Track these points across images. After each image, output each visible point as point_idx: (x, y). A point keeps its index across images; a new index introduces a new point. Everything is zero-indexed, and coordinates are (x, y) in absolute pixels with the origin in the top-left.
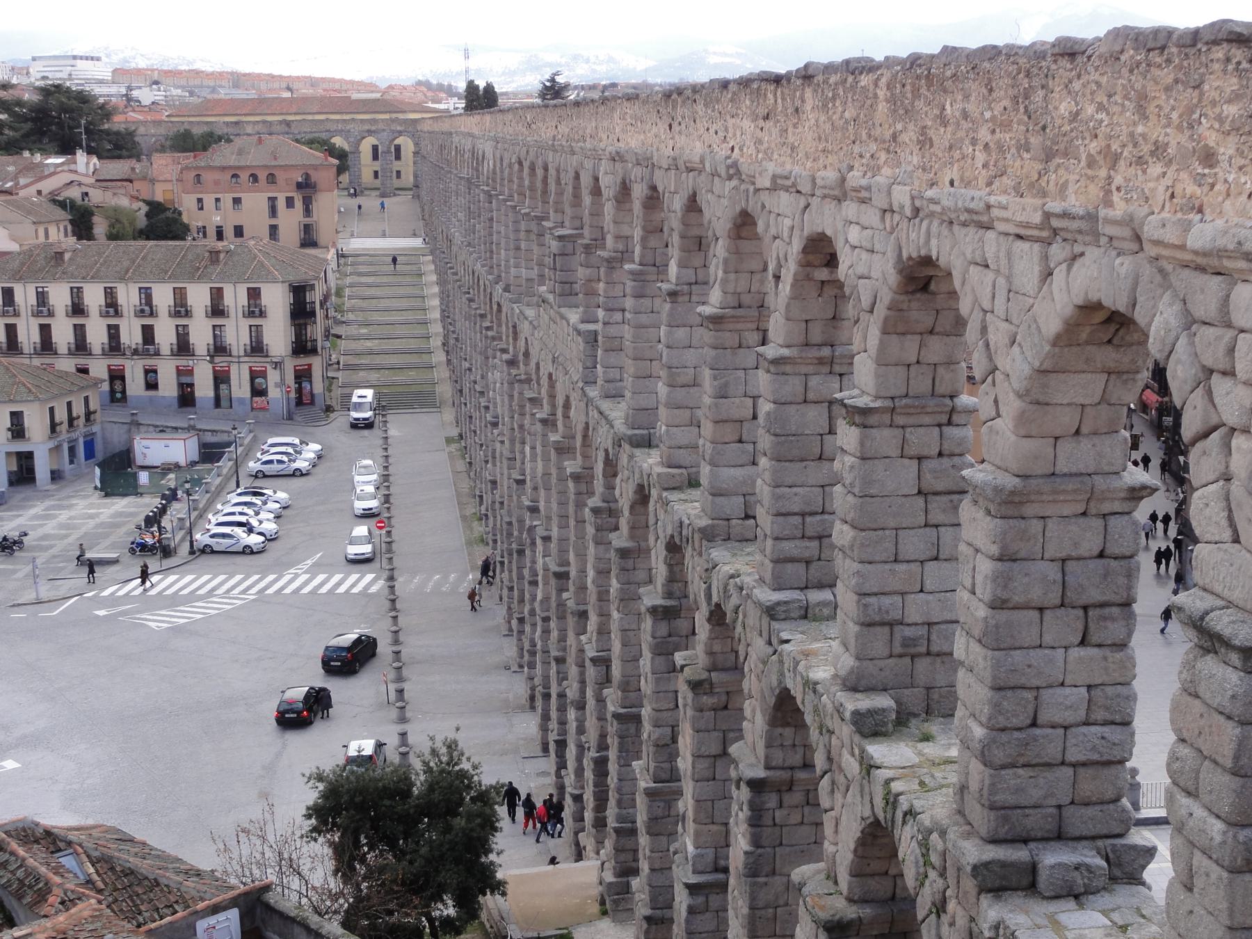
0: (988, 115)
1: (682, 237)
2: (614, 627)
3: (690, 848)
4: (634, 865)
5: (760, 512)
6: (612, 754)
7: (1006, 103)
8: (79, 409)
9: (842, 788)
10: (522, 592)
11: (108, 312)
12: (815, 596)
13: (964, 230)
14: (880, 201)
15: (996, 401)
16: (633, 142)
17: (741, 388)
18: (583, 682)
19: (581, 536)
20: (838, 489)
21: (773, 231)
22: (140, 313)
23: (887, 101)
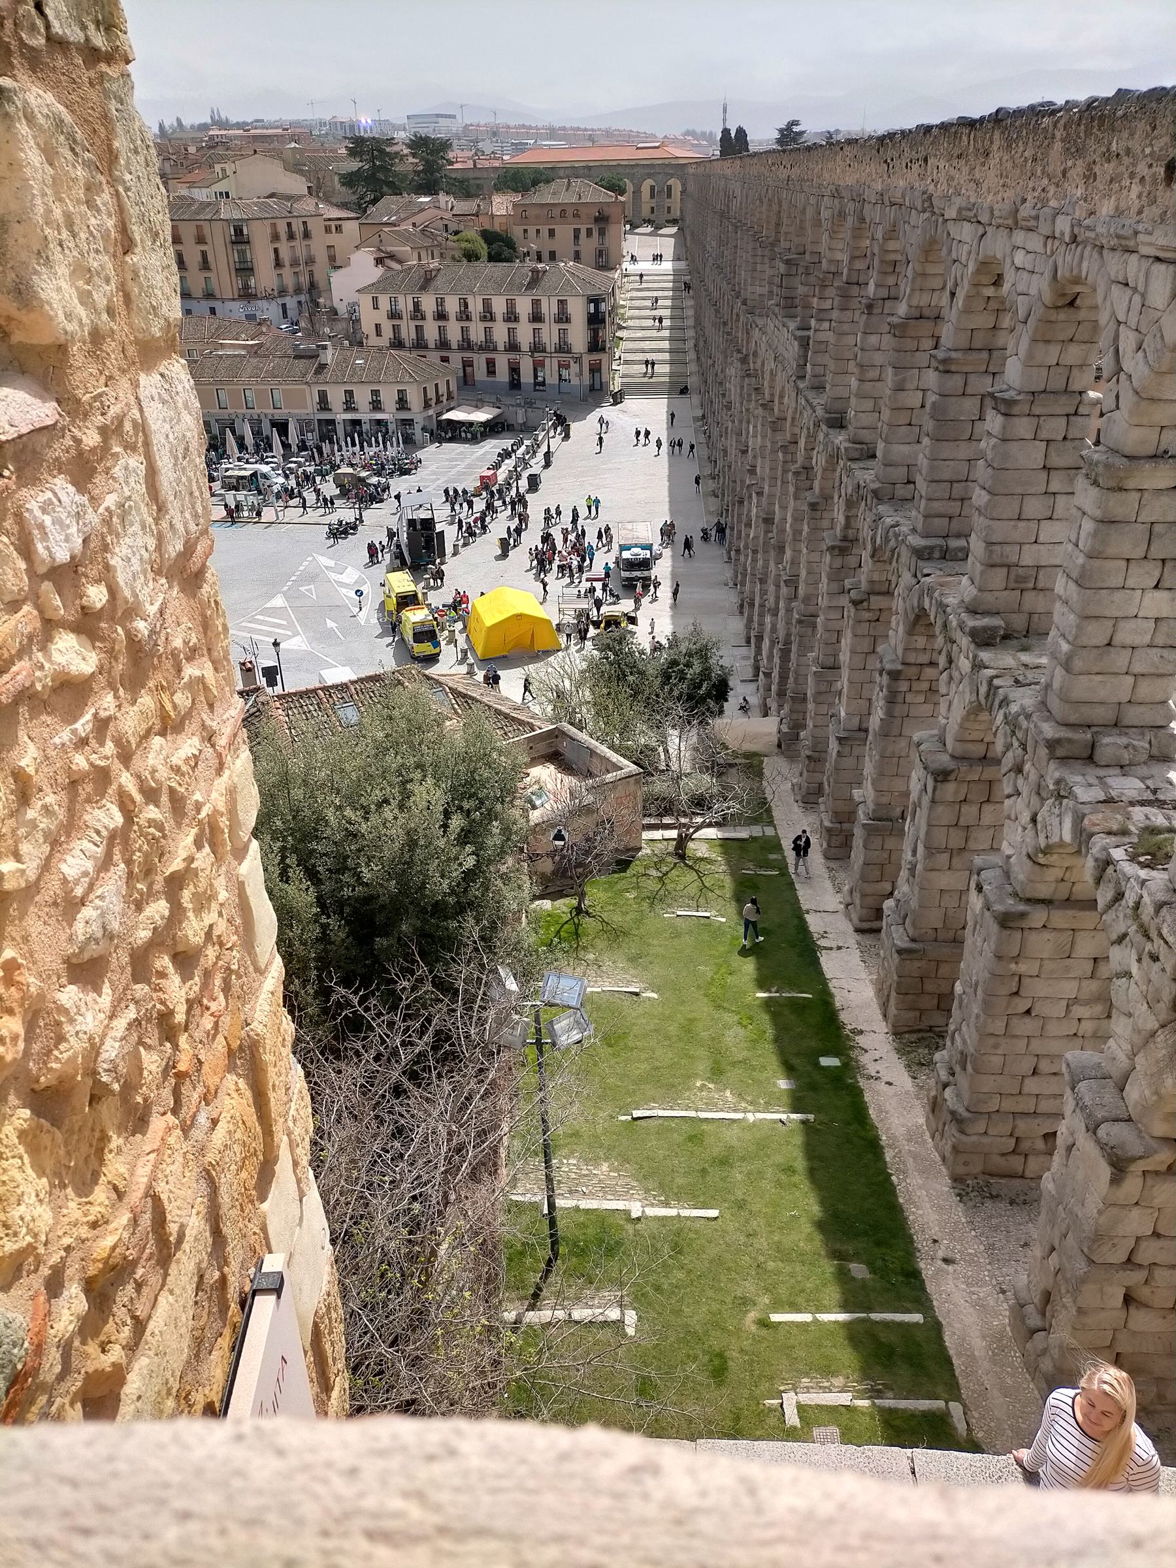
0: (1148, 151)
1: (882, 262)
2: (803, 559)
3: (843, 714)
5: (919, 479)
6: (794, 648)
8: (443, 389)
9: (956, 680)
10: (740, 532)
12: (954, 543)
13: (1111, 254)
14: (1045, 229)
15: (1117, 397)
16: (850, 179)
17: (914, 386)
18: (777, 598)
19: (785, 493)
20: (981, 462)
21: (954, 255)
22: (483, 319)
23: (1063, 140)
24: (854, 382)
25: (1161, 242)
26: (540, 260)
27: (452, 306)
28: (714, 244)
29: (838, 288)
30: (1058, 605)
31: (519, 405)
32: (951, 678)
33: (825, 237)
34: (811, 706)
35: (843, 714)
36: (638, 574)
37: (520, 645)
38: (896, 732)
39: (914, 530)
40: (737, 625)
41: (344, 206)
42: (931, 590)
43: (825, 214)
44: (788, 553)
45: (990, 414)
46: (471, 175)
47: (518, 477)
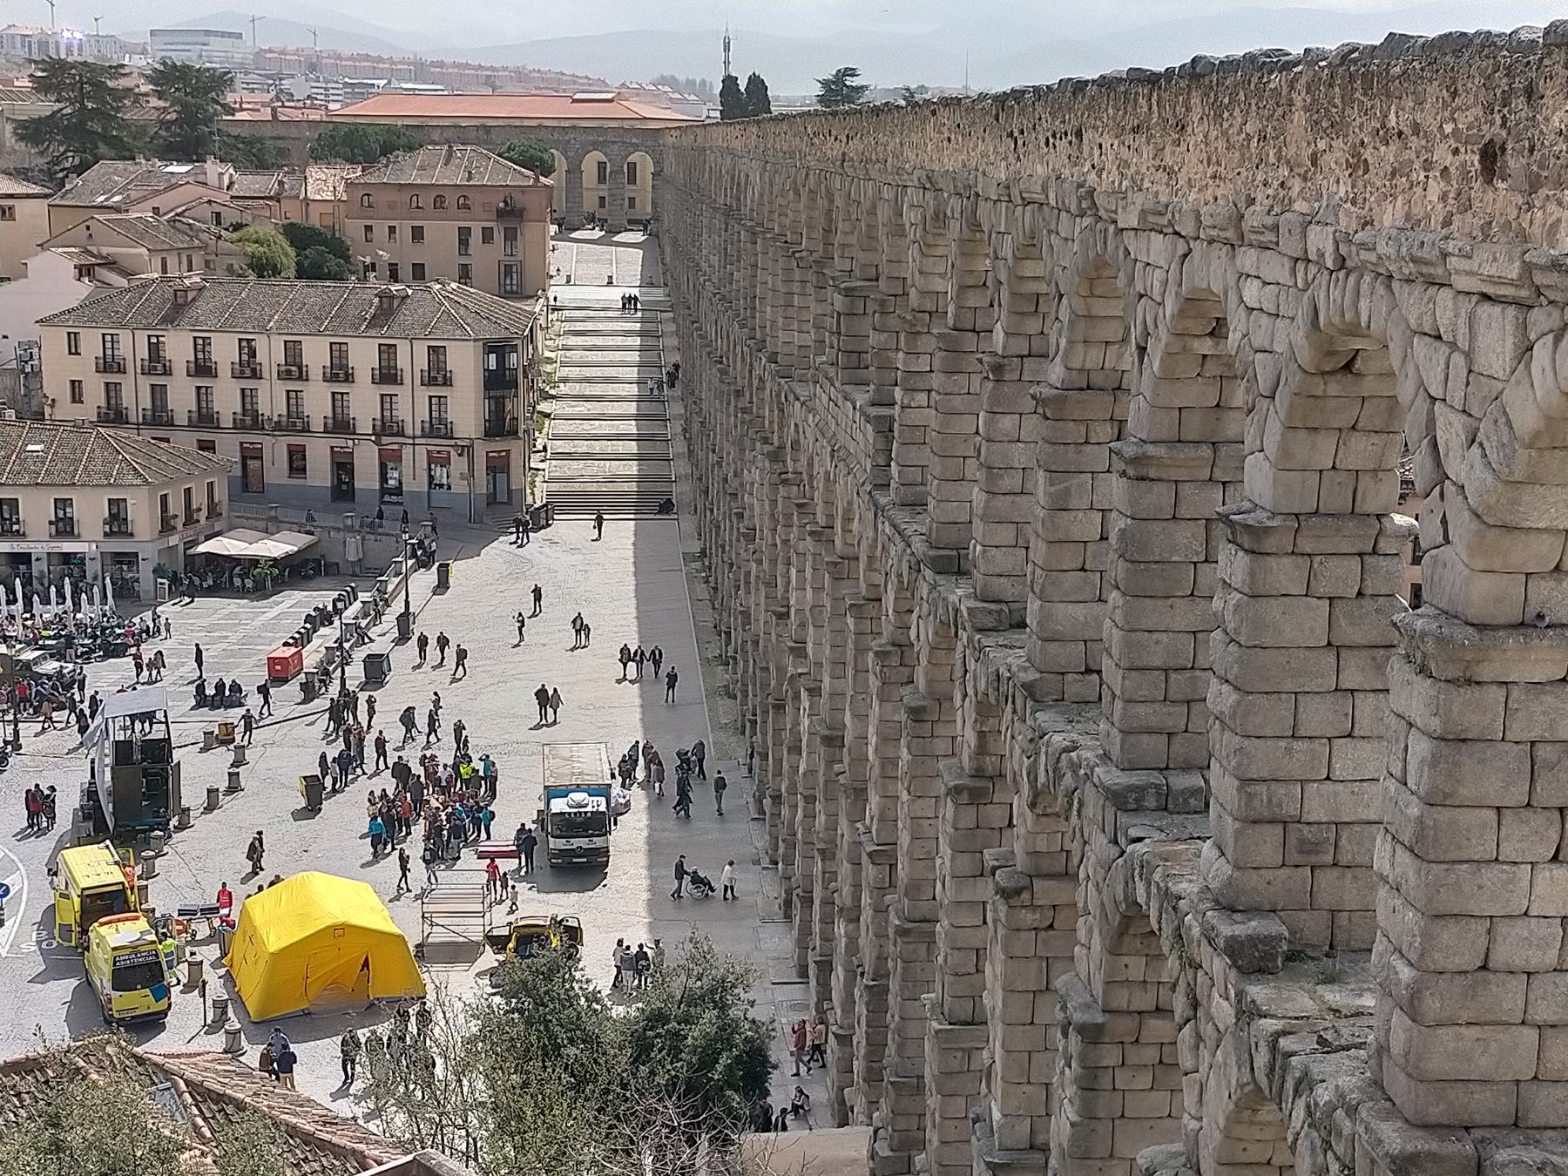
4: (920, 1135)
5: (1106, 664)
6: (894, 984)
7: (1478, 111)
8: (200, 499)
9: (1210, 1043)
11: (242, 372)
12: (1181, 781)
13: (1406, 288)
14: (1290, 246)
18: (857, 887)
19: (861, 690)
20: (1217, 635)
24: (978, 496)
25: (1488, 270)
26: (394, 277)
27: (225, 351)
28: (715, 260)
29: (940, 336)
30: (1383, 892)
31: (350, 529)
32: (1199, 1038)
33: (913, 252)
34: (933, 1101)
35: (997, 1115)
36: (582, 842)
37: (346, 991)
38: (1101, 1150)
39: (1106, 757)
40: (777, 942)
41: (21, 174)
42: (1146, 868)
43: (910, 216)
44: (874, 802)
45: (1225, 552)
46: (267, 132)
47: (345, 662)
